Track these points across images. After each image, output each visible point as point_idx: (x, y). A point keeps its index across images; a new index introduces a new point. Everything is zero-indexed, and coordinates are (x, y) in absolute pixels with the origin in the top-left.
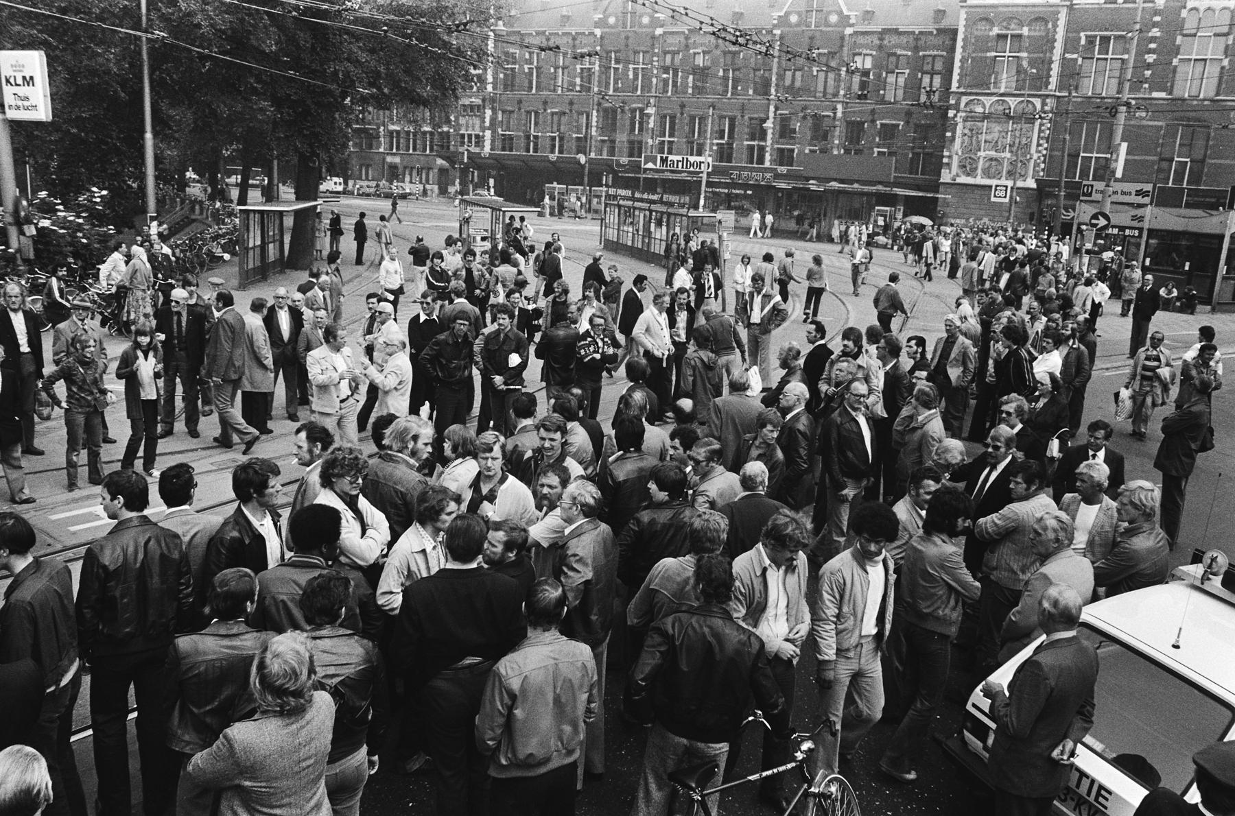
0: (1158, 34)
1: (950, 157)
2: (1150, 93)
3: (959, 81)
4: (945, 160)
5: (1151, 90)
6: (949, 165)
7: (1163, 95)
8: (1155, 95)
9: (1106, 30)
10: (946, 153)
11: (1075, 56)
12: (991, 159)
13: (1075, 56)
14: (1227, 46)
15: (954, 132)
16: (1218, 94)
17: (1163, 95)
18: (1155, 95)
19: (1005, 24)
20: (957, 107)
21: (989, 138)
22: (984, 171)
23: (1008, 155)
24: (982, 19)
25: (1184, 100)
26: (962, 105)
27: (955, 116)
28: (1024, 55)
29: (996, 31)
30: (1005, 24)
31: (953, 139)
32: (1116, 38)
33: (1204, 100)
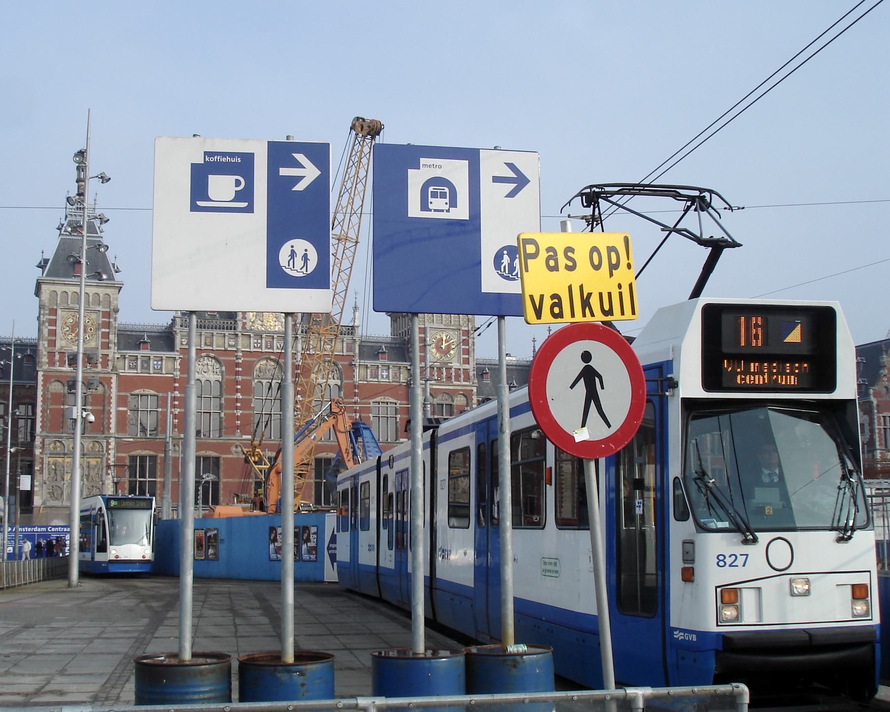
3: (41, 427)
11: (125, 409)
13: (125, 409)
14: (221, 405)
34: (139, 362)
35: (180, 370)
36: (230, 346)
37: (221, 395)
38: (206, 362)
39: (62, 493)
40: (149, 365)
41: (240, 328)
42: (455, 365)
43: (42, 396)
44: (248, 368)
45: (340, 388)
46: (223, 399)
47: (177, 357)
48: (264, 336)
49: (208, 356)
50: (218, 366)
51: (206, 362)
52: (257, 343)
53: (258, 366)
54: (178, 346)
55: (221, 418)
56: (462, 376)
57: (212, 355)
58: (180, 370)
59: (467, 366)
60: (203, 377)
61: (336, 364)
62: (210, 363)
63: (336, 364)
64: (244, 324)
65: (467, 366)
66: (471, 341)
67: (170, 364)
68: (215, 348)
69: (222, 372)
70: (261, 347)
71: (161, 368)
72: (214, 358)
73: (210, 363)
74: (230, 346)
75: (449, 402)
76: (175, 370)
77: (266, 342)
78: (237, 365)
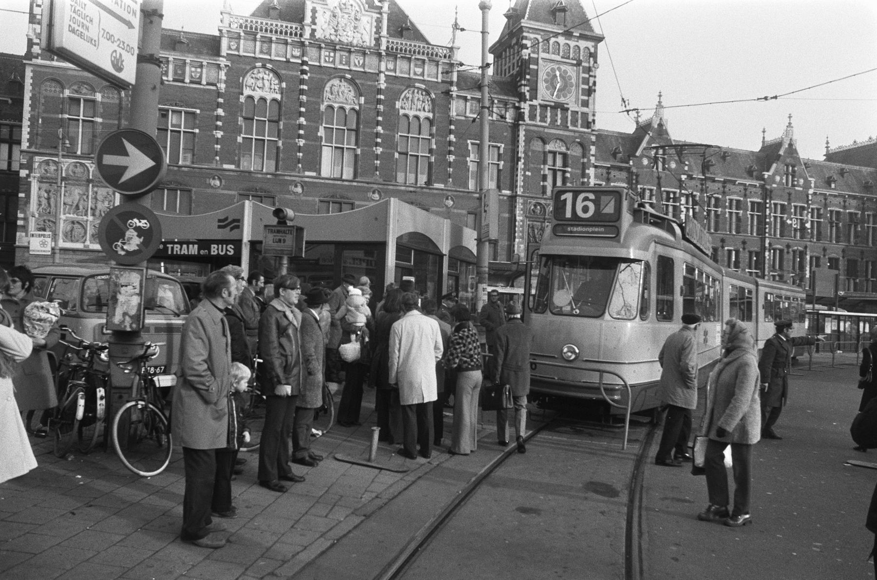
0: (223, 114)
1: (25, 219)
2: (222, 164)
3: (29, 140)
4: (20, 223)
5: (223, 161)
6: (25, 228)
7: (232, 167)
8: (226, 166)
9: (176, 105)
10: (20, 215)
12: (73, 223)
15: (28, 193)
16: (277, 169)
17: (232, 167)
18: (226, 166)
19: (75, 87)
20: (29, 166)
21: (69, 200)
22: (66, 235)
23: (90, 218)
24: (53, 80)
25: (250, 172)
26: (36, 165)
27: (28, 176)
28: (99, 120)
29: (67, 93)
30: (75, 87)
31: (28, 196)
32: (186, 113)
33: (267, 174)
34: (171, 67)
35: (225, 82)
36: (293, 57)
37: (279, 120)
38: (261, 75)
39: (85, 233)
40: (184, 73)
41: (307, 35)
42: (573, 107)
43: (31, 98)
44: (317, 89)
45: (431, 122)
46: (281, 123)
47: (222, 65)
48: (338, 47)
49: (264, 66)
50: (277, 82)
51: (261, 75)
52: (329, 56)
53: (329, 85)
54: (224, 51)
55: (278, 148)
56: (580, 121)
57: (269, 66)
58: (225, 82)
59: (585, 110)
60: (257, 94)
61: (428, 94)
62: (266, 77)
63: (428, 94)
64: (314, 31)
65: (585, 110)
66: (592, 80)
67: (213, 72)
68: (273, 58)
69: (281, 89)
70: (334, 62)
71: (200, 77)
72: (272, 70)
73: (266, 77)
74: (293, 57)
75: (563, 149)
76: (219, 81)
77: (341, 56)
78: (302, 82)
